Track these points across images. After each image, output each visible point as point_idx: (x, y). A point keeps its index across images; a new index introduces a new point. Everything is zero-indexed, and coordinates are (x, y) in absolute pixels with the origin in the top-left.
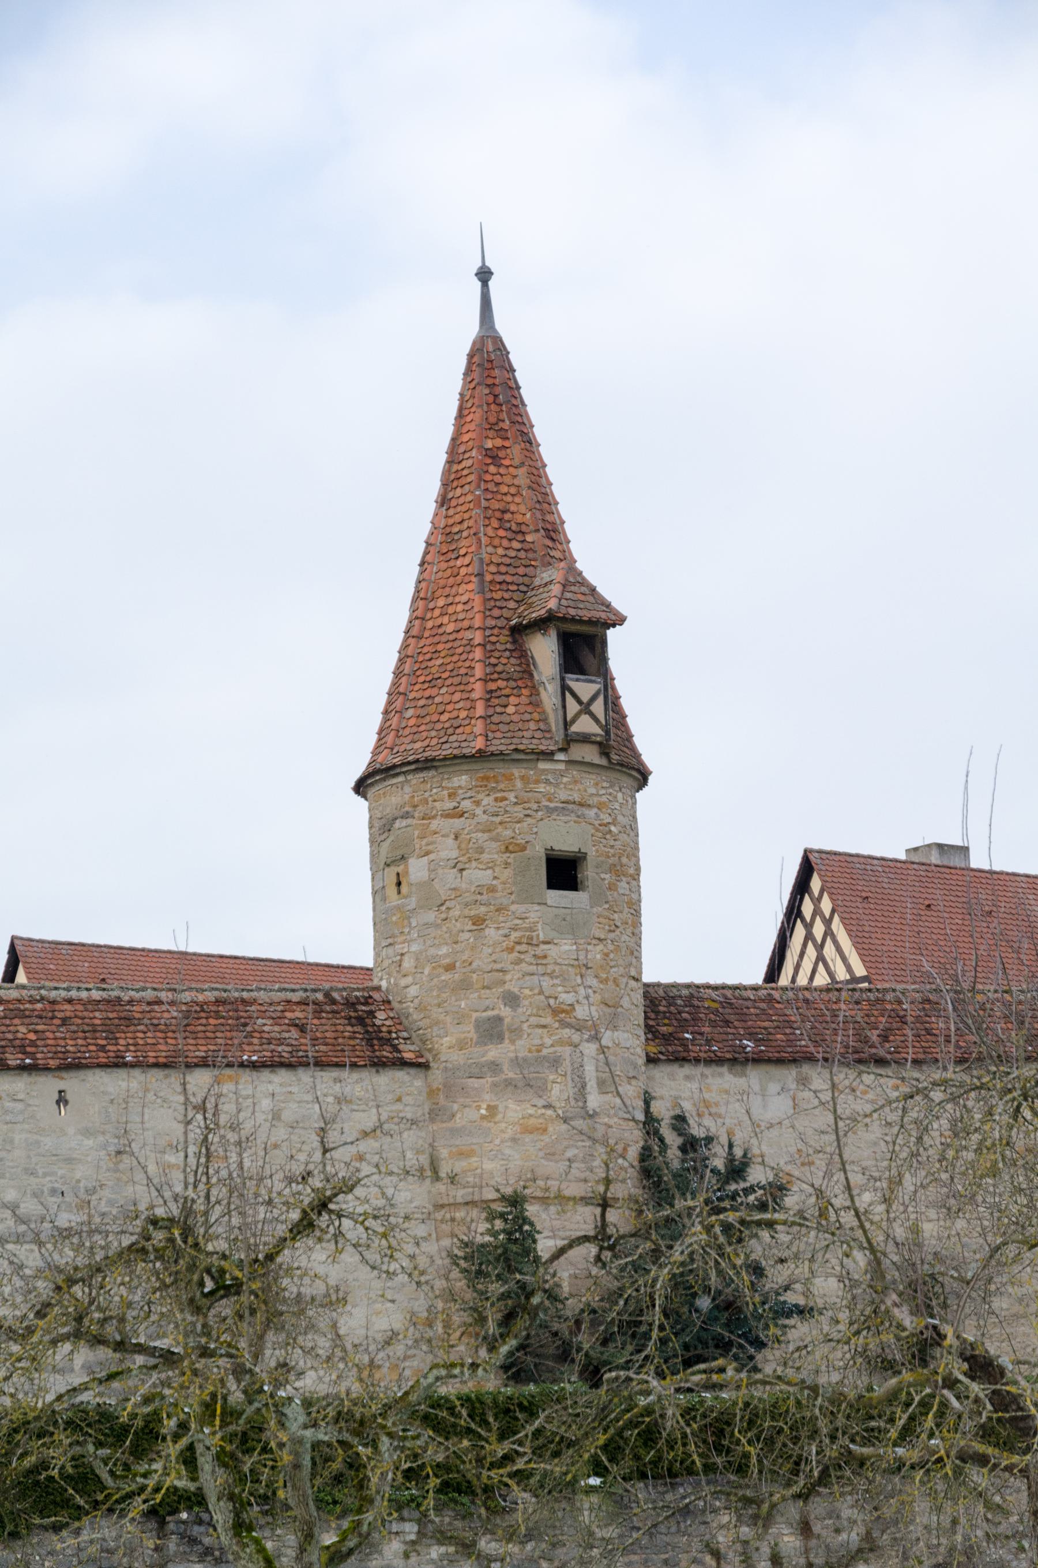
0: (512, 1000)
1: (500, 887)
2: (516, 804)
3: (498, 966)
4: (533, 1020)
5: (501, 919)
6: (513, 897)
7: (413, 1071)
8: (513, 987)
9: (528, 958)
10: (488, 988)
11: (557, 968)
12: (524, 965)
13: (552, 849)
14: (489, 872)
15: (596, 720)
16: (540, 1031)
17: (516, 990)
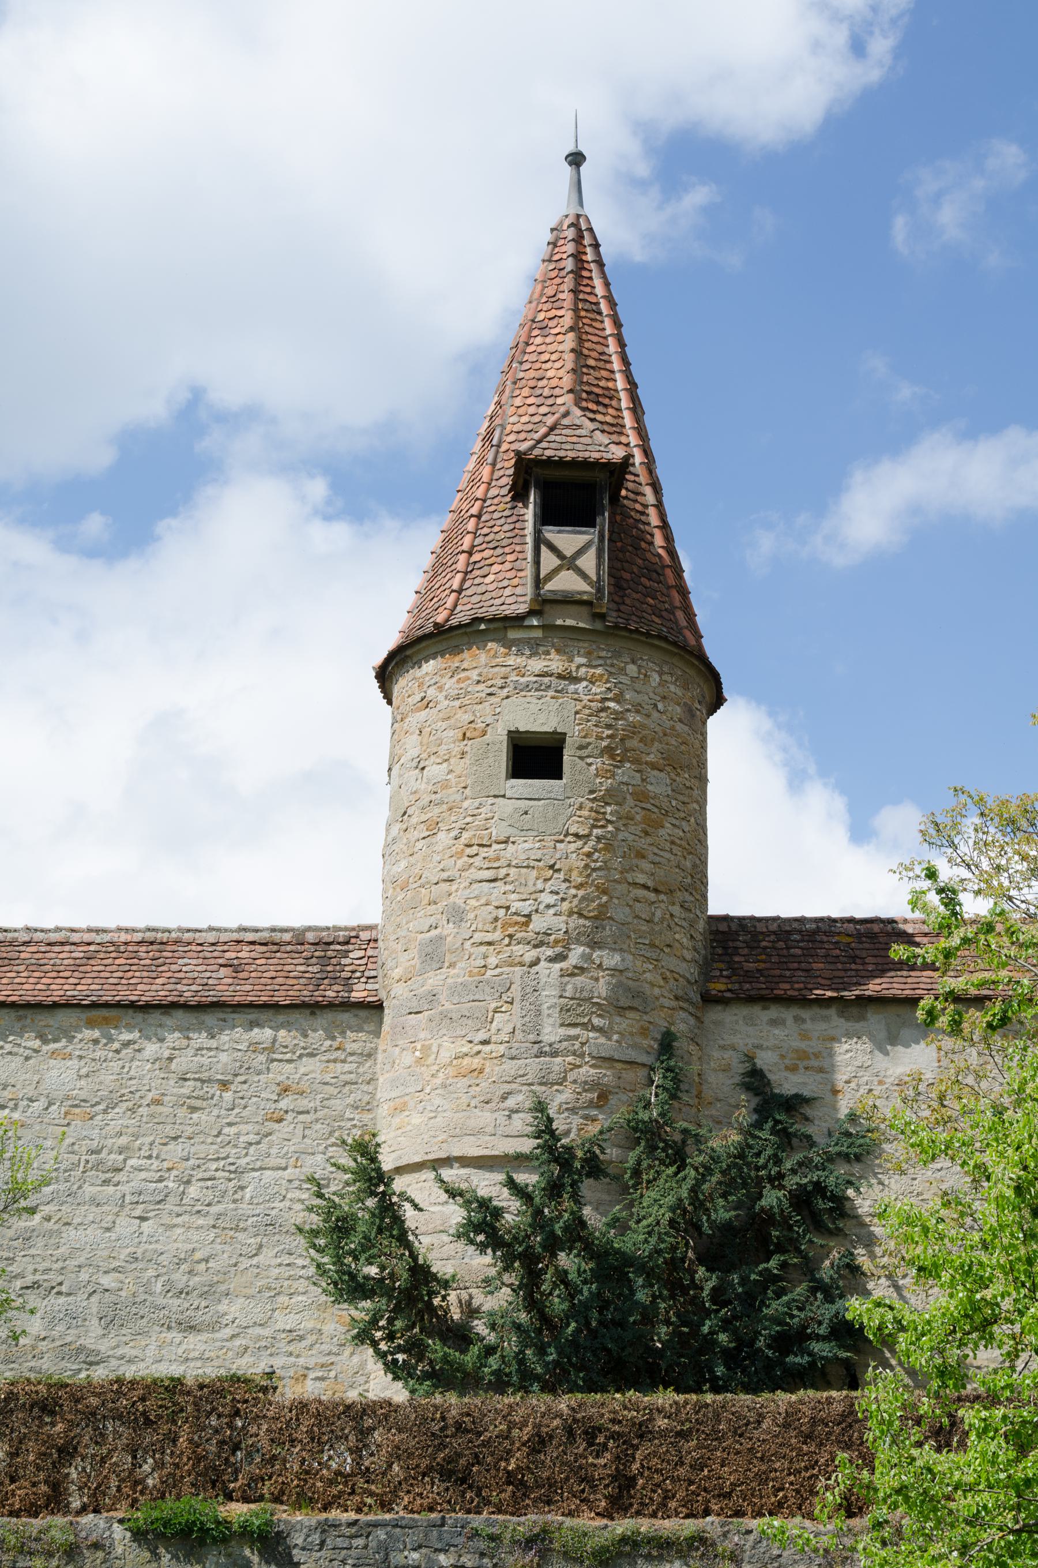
0: (457, 915)
1: (454, 781)
2: (479, 682)
3: (445, 875)
4: (478, 937)
5: (453, 819)
6: (467, 791)
7: (363, 1013)
8: (457, 899)
9: (477, 861)
10: (435, 903)
11: (513, 871)
12: (472, 870)
13: (517, 732)
14: (445, 765)
15: (584, 575)
16: (483, 949)
17: (460, 902)
